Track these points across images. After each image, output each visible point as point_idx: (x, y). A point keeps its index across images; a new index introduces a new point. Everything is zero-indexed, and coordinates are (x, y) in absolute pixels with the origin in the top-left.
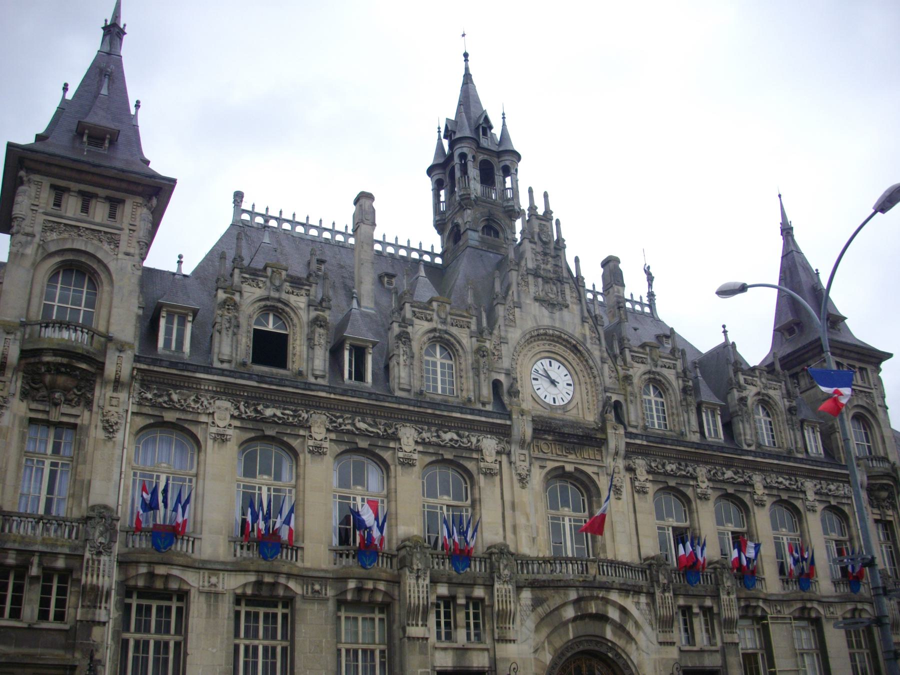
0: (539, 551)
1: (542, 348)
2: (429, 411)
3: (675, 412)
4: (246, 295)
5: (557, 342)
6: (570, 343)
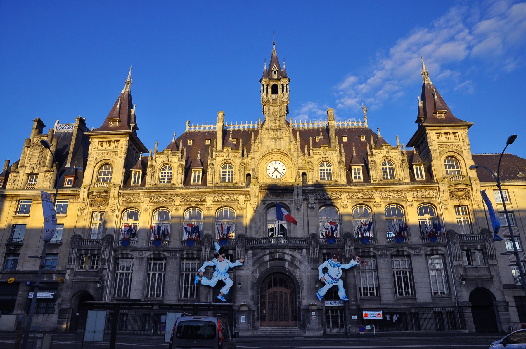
0: (260, 236)
4: (157, 161)
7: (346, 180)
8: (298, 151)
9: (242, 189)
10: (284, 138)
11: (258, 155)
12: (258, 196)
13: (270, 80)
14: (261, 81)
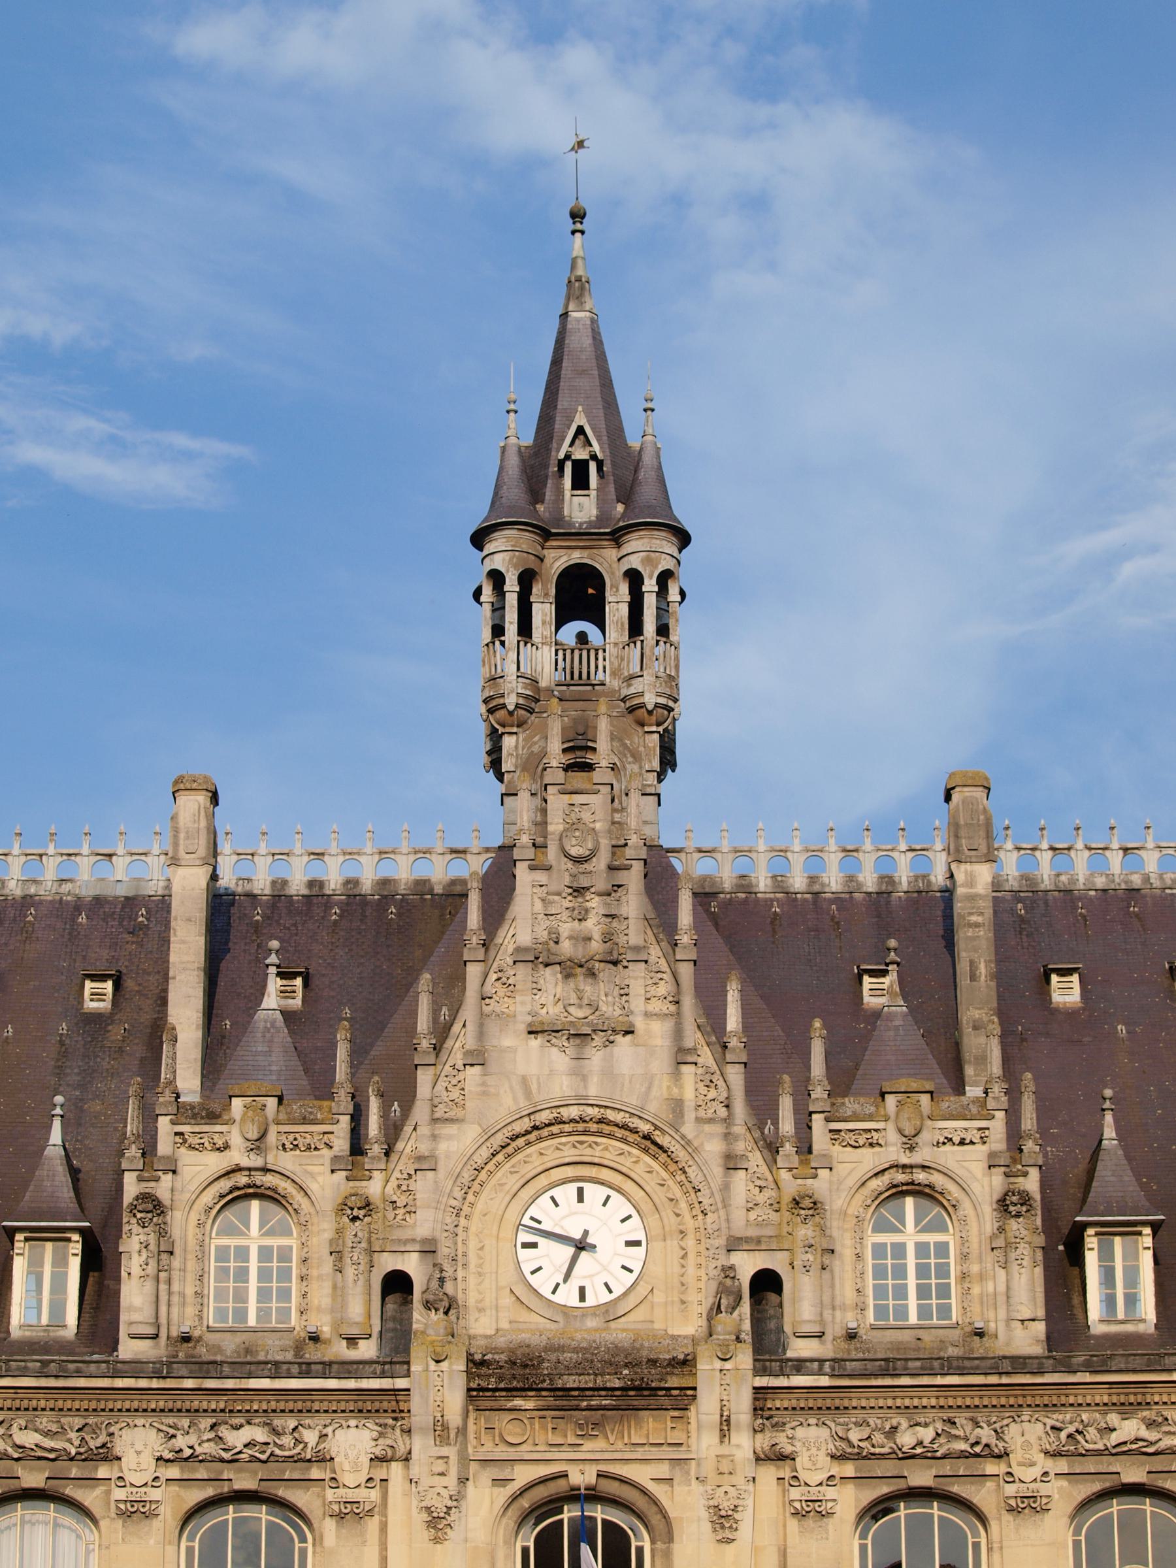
1: (552, 1158)
2: (189, 1383)
3: (975, 1268)
5: (600, 1134)
6: (634, 1131)
7: (1040, 1328)
8: (728, 1121)
9: (351, 1384)
10: (639, 1023)
11: (459, 1144)
12: (462, 1431)
13: (545, 534)
14: (479, 539)
